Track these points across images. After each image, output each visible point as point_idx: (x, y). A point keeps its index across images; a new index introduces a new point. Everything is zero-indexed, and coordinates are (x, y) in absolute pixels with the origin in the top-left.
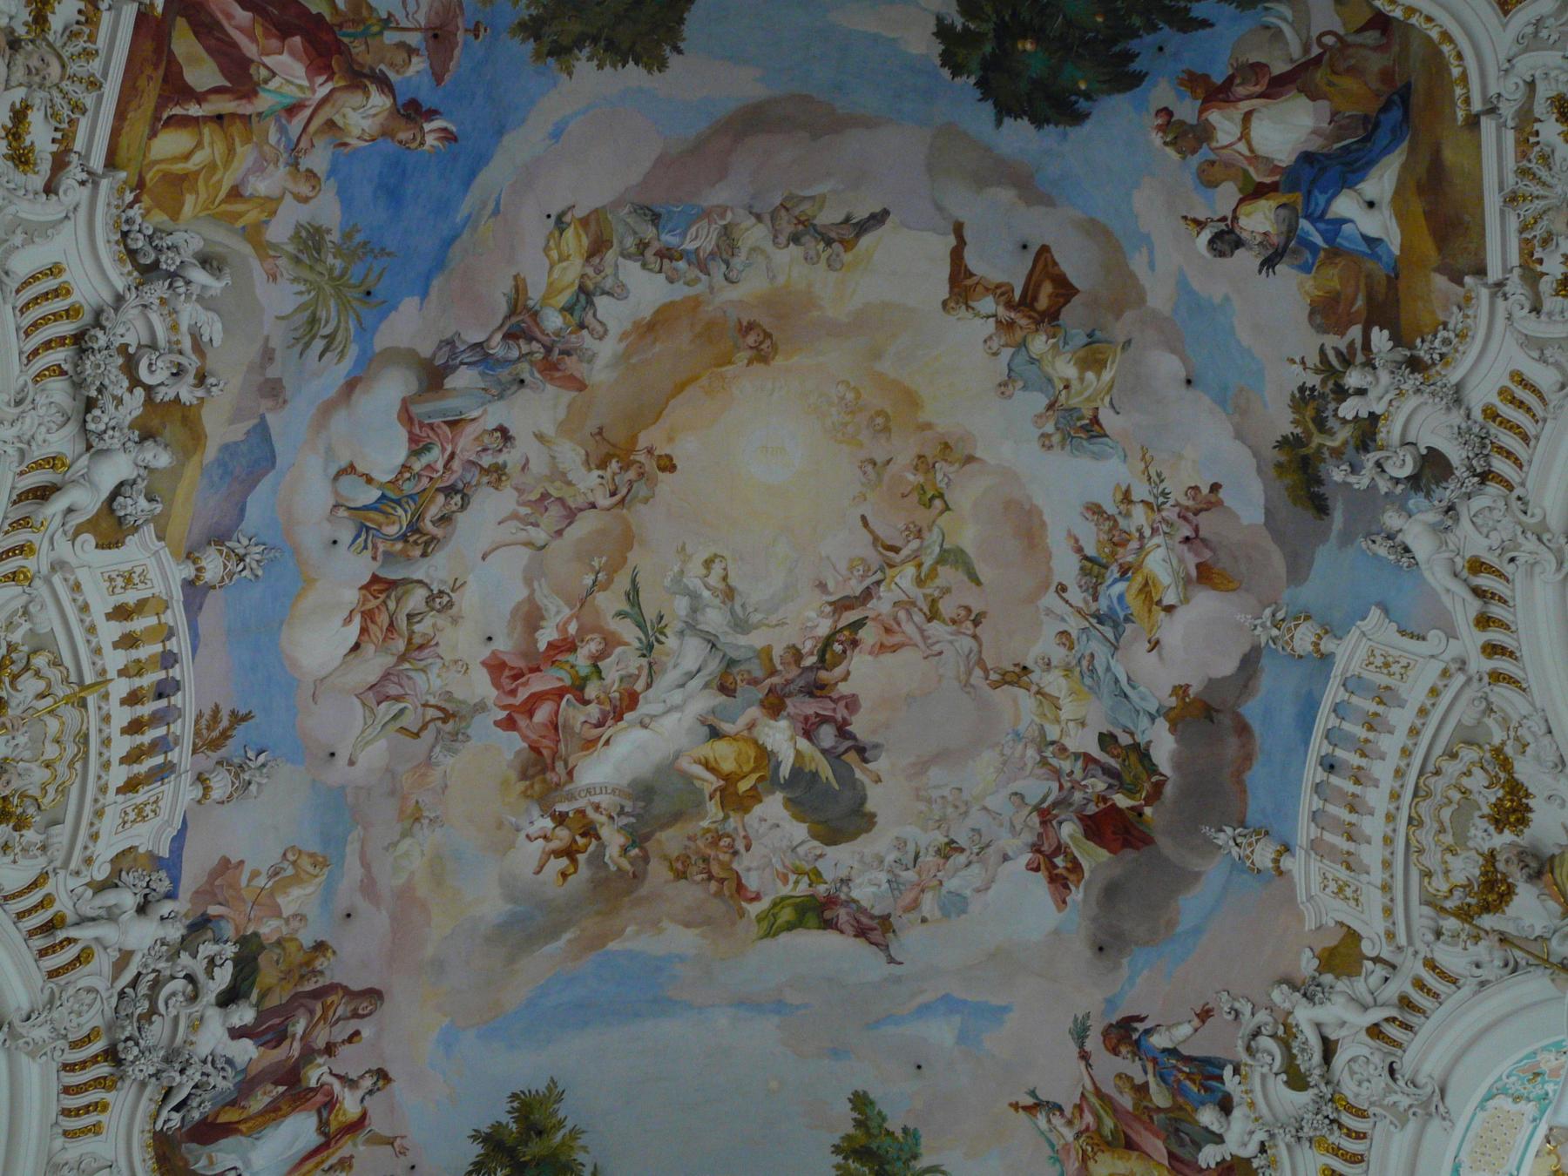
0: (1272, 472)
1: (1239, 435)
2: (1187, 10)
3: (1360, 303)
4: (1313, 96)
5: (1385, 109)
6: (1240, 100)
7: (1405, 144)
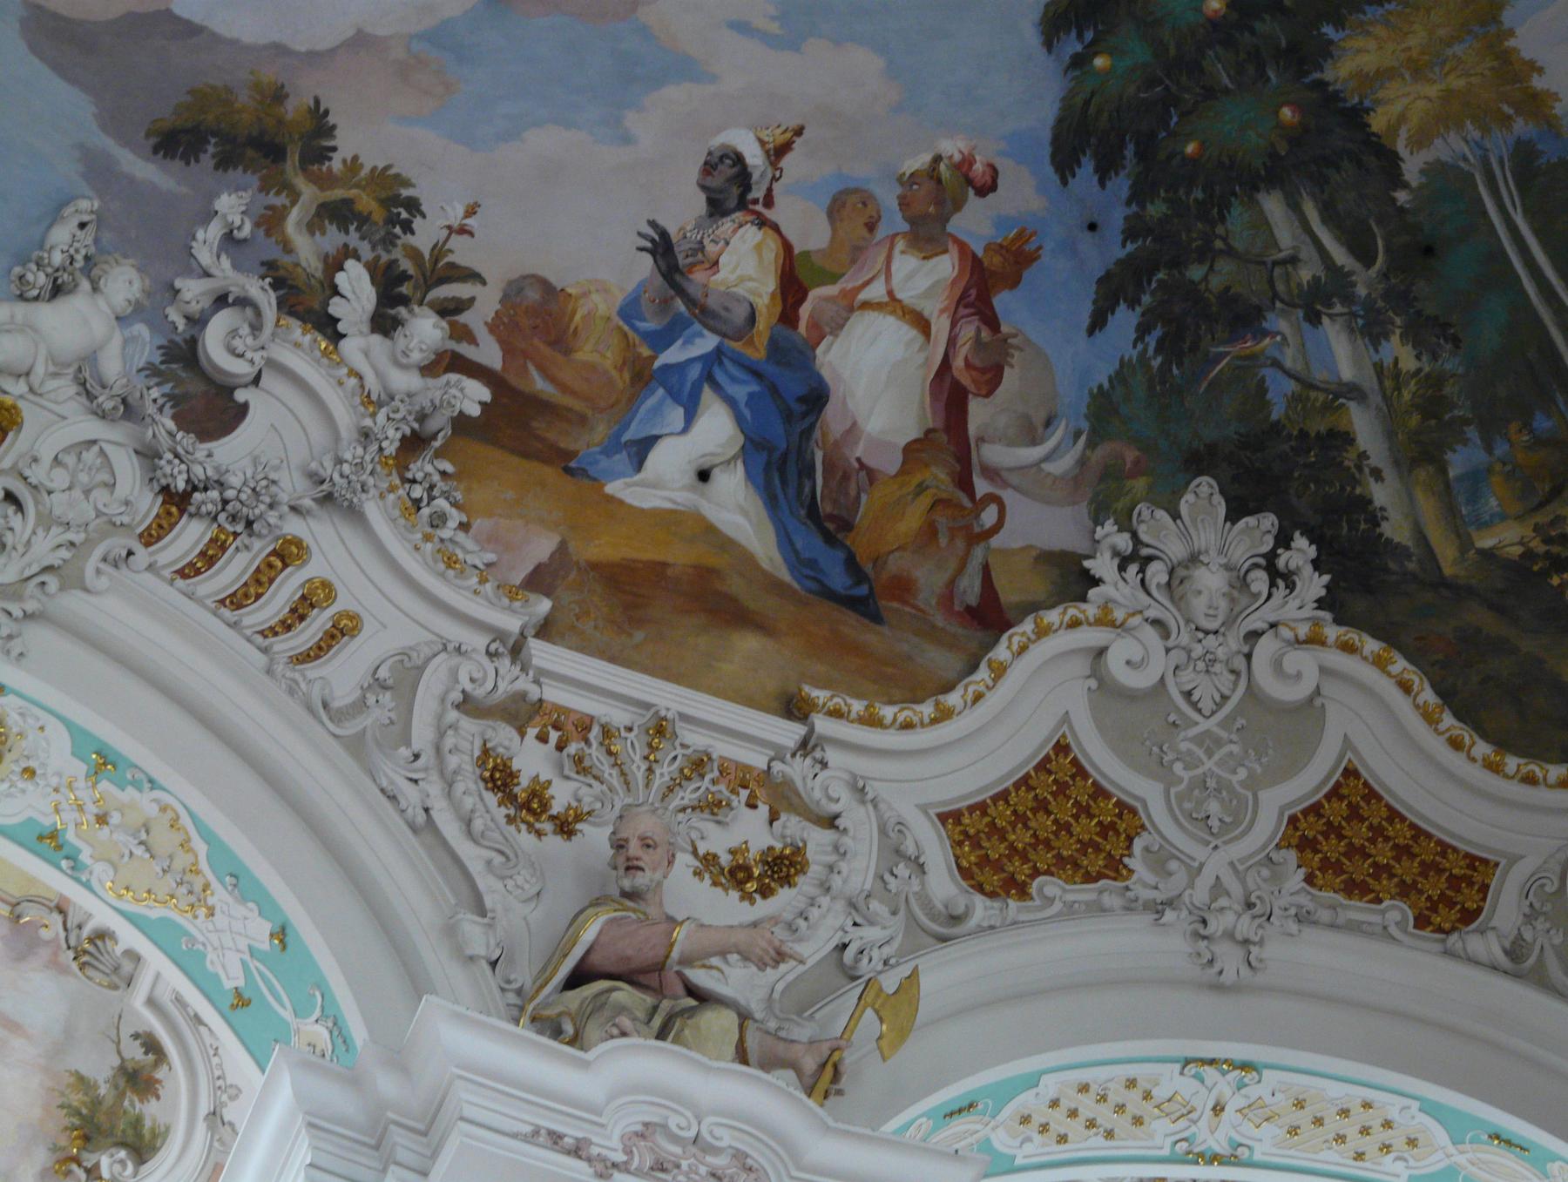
0: (270, 74)
1: (360, 41)
2: (1133, 303)
3: (540, 385)
4: (910, 450)
5: (851, 564)
6: (953, 324)
7: (785, 575)
